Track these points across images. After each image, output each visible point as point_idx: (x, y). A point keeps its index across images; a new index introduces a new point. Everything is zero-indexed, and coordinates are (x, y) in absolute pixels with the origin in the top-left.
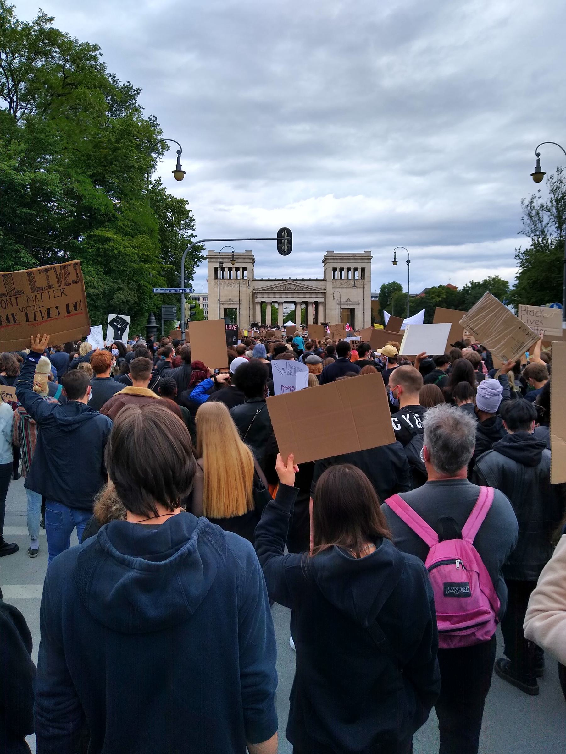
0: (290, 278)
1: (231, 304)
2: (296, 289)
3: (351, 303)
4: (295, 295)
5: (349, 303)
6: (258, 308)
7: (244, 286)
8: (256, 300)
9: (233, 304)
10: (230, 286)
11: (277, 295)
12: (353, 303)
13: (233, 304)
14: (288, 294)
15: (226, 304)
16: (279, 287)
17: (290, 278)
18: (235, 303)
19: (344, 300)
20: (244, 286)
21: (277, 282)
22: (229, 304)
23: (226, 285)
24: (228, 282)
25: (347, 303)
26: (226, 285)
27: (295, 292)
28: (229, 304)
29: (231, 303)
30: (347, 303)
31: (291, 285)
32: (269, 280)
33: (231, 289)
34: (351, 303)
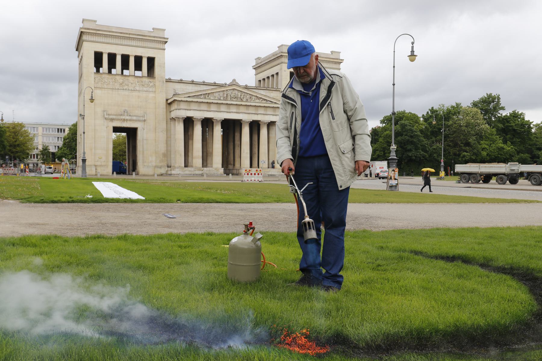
0: (234, 80)
1: (127, 120)
2: (244, 100)
4: (242, 109)
6: (180, 128)
7: (151, 89)
8: (173, 115)
9: (130, 120)
10: (126, 87)
11: (213, 108)
13: (130, 120)
14: (231, 107)
15: (118, 120)
16: (217, 95)
17: (234, 80)
18: (135, 118)
21: (205, 88)
22: (124, 120)
23: (117, 86)
24: (121, 81)
26: (117, 86)
28: (124, 120)
29: (128, 118)
31: (236, 92)
32: (192, 83)
33: (126, 93)
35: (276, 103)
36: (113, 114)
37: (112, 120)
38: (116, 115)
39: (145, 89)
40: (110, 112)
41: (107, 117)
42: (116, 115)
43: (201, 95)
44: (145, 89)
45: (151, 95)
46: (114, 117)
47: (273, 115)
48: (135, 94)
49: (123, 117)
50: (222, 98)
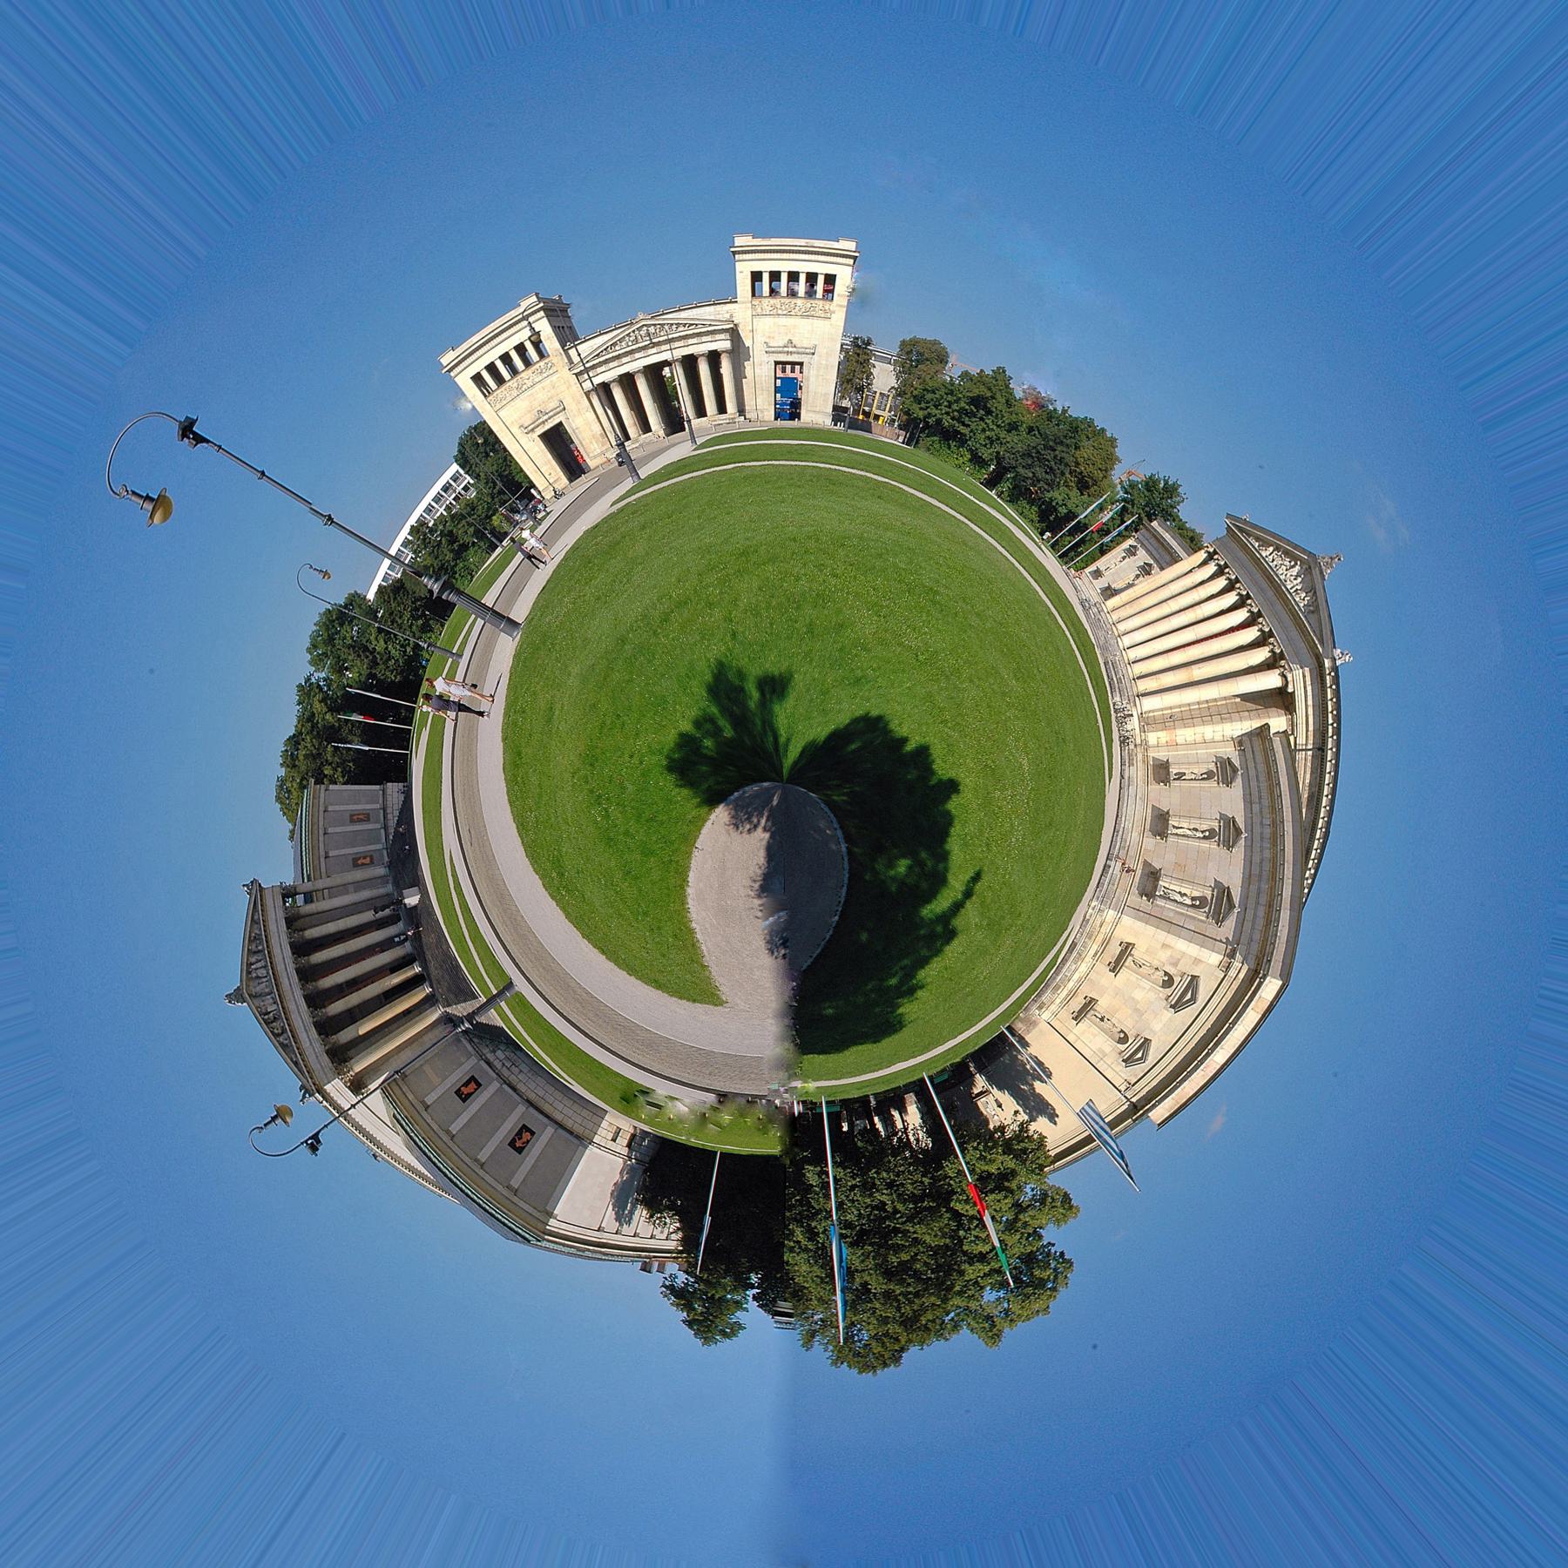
3: (794, 349)
5: (791, 349)
7: (551, 372)
10: (525, 387)
12: (800, 350)
15: (538, 426)
19: (780, 341)
20: (551, 372)
25: (786, 349)
27: (661, 339)
30: (786, 349)
34: (794, 349)
35: (710, 325)
36: (529, 423)
37: (533, 430)
38: (532, 424)
39: (545, 375)
40: (526, 425)
41: (526, 431)
42: (532, 424)
43: (602, 352)
44: (545, 375)
45: (554, 378)
46: (532, 426)
47: (712, 341)
48: (538, 387)
49: (541, 420)
50: (630, 344)
